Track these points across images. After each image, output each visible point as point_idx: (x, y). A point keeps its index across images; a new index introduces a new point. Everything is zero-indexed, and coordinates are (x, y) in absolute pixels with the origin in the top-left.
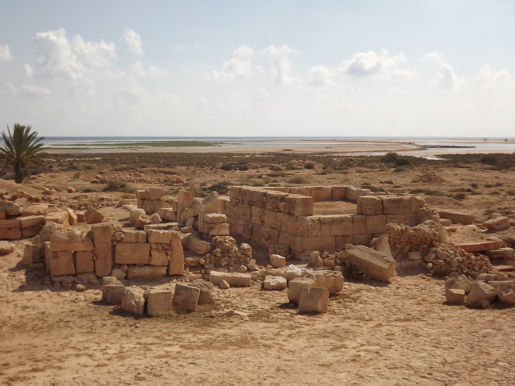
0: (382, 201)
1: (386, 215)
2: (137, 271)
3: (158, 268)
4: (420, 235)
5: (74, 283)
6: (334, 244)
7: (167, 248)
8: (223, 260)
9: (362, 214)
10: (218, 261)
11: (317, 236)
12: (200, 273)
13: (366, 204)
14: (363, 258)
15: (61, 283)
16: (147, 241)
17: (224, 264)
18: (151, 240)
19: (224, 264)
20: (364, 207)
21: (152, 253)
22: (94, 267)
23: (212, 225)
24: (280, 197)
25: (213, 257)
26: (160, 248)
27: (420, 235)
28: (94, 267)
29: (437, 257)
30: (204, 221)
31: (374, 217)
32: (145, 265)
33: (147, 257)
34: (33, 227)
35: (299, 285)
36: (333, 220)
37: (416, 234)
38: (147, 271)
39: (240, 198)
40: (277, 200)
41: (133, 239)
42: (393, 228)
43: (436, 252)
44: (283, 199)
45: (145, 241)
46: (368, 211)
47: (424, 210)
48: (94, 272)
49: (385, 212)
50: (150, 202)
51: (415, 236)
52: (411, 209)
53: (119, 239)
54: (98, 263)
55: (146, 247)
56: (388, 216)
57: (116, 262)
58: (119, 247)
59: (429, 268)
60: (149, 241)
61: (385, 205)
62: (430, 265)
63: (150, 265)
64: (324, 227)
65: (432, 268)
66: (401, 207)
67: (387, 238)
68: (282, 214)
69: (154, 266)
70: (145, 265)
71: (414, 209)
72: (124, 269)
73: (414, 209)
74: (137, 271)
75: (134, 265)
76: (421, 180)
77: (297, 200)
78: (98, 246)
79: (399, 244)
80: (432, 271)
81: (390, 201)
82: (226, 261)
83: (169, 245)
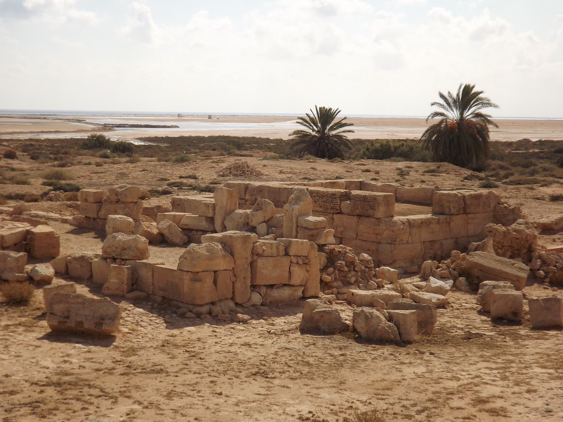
0: (464, 197)
1: (467, 214)
2: (276, 294)
3: (297, 288)
4: (524, 237)
5: (233, 312)
6: (423, 251)
7: (305, 262)
8: (350, 275)
9: (443, 214)
10: (345, 277)
11: (408, 243)
12: (332, 293)
13: (449, 202)
14: (491, 266)
15: (210, 313)
16: (287, 254)
17: (353, 280)
18: (292, 251)
19: (353, 280)
20: (446, 204)
21: (292, 269)
22: (233, 292)
23: (315, 231)
24: (338, 194)
25: (337, 272)
26: (301, 262)
27: (524, 237)
28: (233, 292)
29: (544, 262)
30: (298, 226)
31: (457, 216)
32: (285, 285)
33: (287, 274)
34: (15, 244)
35: (510, 297)
36: (422, 223)
37: (519, 236)
38: (286, 293)
39: (247, 197)
40: (335, 198)
41: (274, 251)
42: (497, 230)
43: (540, 257)
44: (346, 196)
45: (284, 253)
46: (452, 209)
47: (506, 207)
48: (233, 299)
49: (468, 210)
50: (122, 205)
51: (517, 239)
52: (490, 207)
53: (260, 251)
54: (238, 285)
55: (286, 261)
56: (469, 216)
57: (257, 282)
58: (260, 262)
59: (543, 277)
60: (290, 254)
61: (468, 202)
62: (542, 272)
63: (289, 285)
64: (414, 230)
65: (546, 277)
66: (481, 204)
67: (491, 242)
68: (344, 217)
69: (293, 286)
70: (285, 285)
71: (492, 206)
72: (262, 292)
73: (492, 206)
74: (276, 294)
75: (272, 286)
76: (230, 173)
77: (377, 197)
78: (238, 262)
79: (501, 249)
80: (548, 280)
81: (471, 196)
82: (353, 276)
83: (306, 257)
